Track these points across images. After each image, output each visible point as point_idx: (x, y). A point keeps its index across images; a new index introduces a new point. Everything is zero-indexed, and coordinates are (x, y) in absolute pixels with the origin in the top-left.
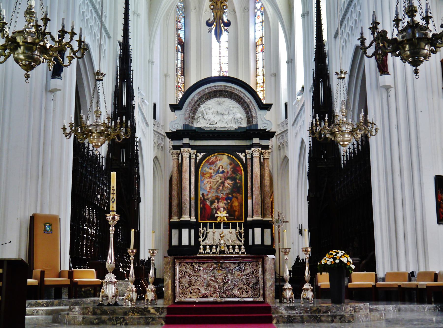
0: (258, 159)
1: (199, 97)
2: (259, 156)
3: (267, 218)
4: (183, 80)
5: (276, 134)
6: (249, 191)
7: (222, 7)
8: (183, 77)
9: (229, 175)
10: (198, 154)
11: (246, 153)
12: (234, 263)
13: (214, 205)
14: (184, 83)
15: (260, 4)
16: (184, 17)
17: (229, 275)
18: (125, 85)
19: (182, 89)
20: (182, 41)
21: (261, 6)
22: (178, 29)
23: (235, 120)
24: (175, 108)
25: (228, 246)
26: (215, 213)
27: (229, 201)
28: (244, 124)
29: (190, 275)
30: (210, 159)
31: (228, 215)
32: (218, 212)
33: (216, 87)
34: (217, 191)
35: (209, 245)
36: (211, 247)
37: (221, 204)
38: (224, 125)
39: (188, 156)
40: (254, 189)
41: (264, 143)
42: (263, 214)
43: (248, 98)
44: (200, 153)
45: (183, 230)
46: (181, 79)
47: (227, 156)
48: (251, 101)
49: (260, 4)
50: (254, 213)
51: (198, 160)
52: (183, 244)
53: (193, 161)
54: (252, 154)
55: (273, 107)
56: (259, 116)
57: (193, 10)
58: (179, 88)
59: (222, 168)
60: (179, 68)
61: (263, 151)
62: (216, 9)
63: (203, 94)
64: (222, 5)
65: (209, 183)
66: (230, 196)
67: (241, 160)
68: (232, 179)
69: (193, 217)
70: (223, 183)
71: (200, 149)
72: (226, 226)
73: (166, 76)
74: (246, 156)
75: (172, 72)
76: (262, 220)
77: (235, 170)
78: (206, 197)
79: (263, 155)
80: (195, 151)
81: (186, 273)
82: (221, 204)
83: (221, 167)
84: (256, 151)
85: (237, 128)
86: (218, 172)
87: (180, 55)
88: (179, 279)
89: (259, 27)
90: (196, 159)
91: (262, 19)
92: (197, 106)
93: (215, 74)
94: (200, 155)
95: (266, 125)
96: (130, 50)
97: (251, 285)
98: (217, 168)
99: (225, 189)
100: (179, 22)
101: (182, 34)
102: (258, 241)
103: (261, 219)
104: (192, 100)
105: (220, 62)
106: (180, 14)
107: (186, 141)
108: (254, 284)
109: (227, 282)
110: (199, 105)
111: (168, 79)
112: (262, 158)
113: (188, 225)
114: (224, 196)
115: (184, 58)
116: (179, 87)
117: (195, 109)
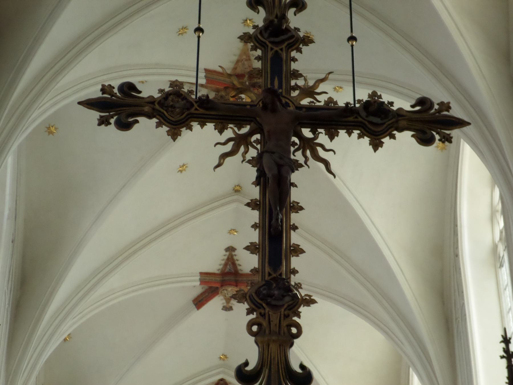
7: (286, 329)
62: (267, 331)
64: (284, 323)
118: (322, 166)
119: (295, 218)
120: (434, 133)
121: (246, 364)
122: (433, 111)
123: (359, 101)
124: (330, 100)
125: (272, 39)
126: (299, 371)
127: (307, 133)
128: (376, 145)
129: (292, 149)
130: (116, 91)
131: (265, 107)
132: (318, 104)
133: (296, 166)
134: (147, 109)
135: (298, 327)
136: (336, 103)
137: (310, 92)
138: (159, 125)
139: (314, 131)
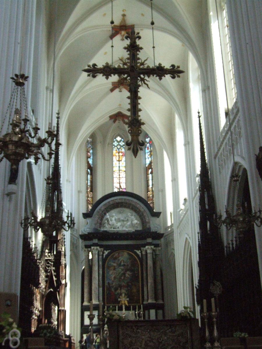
0: (151, 255)
1: (105, 207)
2: (152, 252)
3: (161, 302)
4: (92, 195)
5: (165, 235)
6: (145, 280)
8: (91, 193)
9: (128, 268)
10: (105, 251)
11: (142, 250)
12: (167, 326)
13: (117, 292)
14: (92, 198)
15: (149, 139)
16: (92, 149)
17: (163, 336)
19: (91, 202)
20: (91, 166)
21: (149, 140)
22: (88, 157)
23: (132, 225)
24: (86, 215)
26: (118, 297)
27: (129, 288)
28: (140, 228)
29: (130, 336)
30: (114, 255)
31: (128, 299)
32: (120, 297)
33: (118, 200)
34: (120, 281)
37: (123, 291)
38: (124, 229)
39: (97, 253)
40: (149, 278)
41: (156, 242)
42: (156, 298)
43: (143, 208)
44: (106, 251)
46: (90, 195)
47: (127, 253)
48: (145, 210)
49: (149, 139)
50: (149, 297)
51: (104, 256)
53: (101, 257)
54: (146, 251)
55: (161, 215)
56: (151, 222)
57: (99, 144)
58: (89, 201)
59: (123, 262)
60: (88, 186)
61: (155, 248)
63: (108, 205)
65: (113, 274)
66: (130, 284)
68: (131, 270)
69: (101, 301)
70: (124, 274)
71: (106, 247)
73: (79, 192)
74: (141, 252)
75: (84, 189)
76: (155, 303)
77: (134, 263)
78: (111, 285)
79: (155, 251)
80: (103, 249)
81: (127, 335)
82: (123, 291)
83: (122, 262)
84: (149, 249)
85: (134, 231)
86: (120, 265)
87: (89, 176)
88: (122, 340)
89: (147, 155)
90: (103, 255)
91: (151, 149)
92: (104, 215)
93: (116, 190)
94: (106, 252)
95: (156, 228)
96: (60, 169)
97: (181, 344)
98: (119, 262)
99: (126, 279)
100: (89, 152)
101: (91, 161)
103: (154, 302)
104: (100, 210)
105: (120, 182)
106: (89, 146)
107: (96, 241)
108: (183, 343)
109: (161, 342)
110: (105, 214)
111: (81, 194)
112: (154, 254)
113: (96, 307)
114: (125, 285)
115: (92, 178)
116: (89, 200)
117: (102, 217)
118: (146, 85)
119: (139, 101)
120: (175, 75)
121: (128, 141)
122: (175, 68)
123: (156, 66)
124: (148, 66)
125: (132, 49)
126: (141, 142)
128: (160, 79)
129: (138, 81)
130: (91, 66)
131: (131, 71)
132: (145, 67)
133: (140, 86)
134: (100, 71)
135: (141, 131)
136: (149, 67)
137: (142, 64)
138: (103, 76)
139: (144, 76)
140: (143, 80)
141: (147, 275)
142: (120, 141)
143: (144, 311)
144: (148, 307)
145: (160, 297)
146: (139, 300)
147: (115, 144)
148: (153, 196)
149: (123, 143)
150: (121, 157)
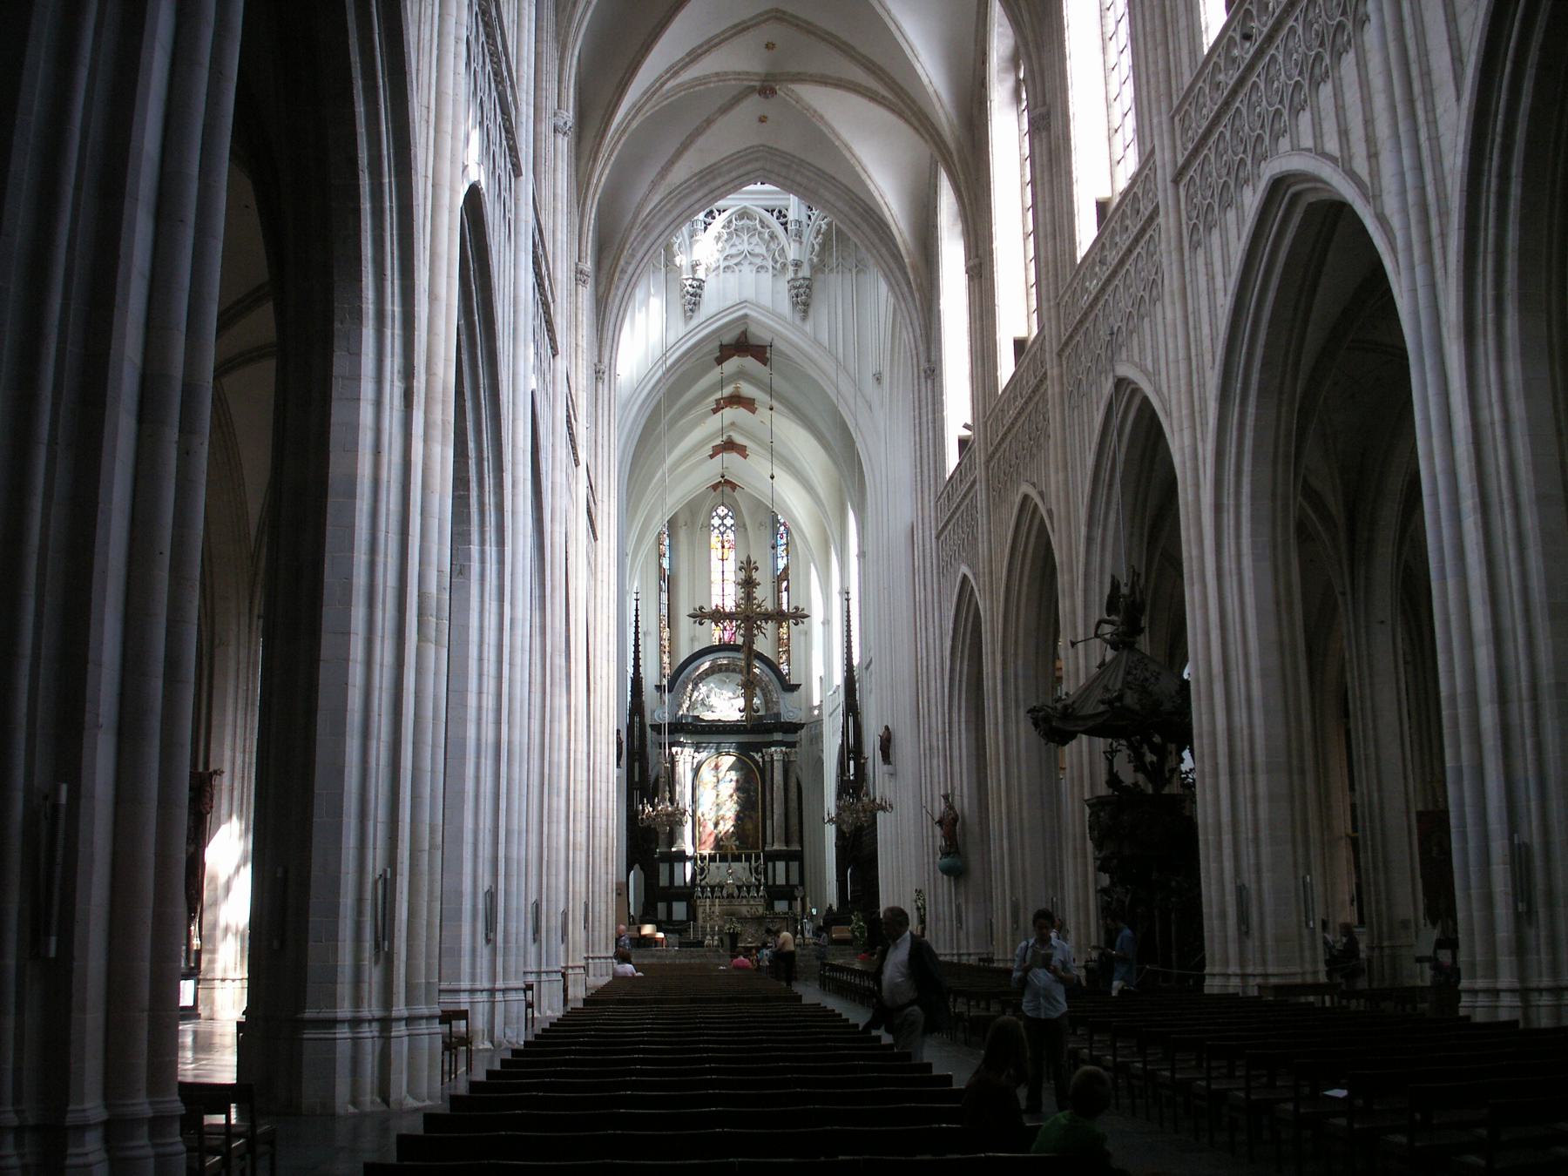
0: (781, 763)
3: (795, 847)
6: (769, 808)
18: (637, 719)
22: (661, 556)
25: (739, 888)
35: (711, 887)
36: (713, 888)
40: (775, 806)
41: (790, 738)
45: (676, 864)
52: (676, 884)
67: (756, 763)
72: (737, 859)
74: (763, 757)
84: (776, 752)
87: (664, 596)
101: (666, 564)
102: (781, 880)
103: (785, 848)
124: (766, 609)
127: (759, 623)
133: (755, 635)
137: (759, 606)
140: (759, 627)
141: (772, 799)
142: (727, 515)
143: (765, 863)
144: (773, 857)
145: (796, 837)
146: (758, 843)
147: (716, 522)
148: (789, 638)
149: (732, 522)
150: (726, 550)
